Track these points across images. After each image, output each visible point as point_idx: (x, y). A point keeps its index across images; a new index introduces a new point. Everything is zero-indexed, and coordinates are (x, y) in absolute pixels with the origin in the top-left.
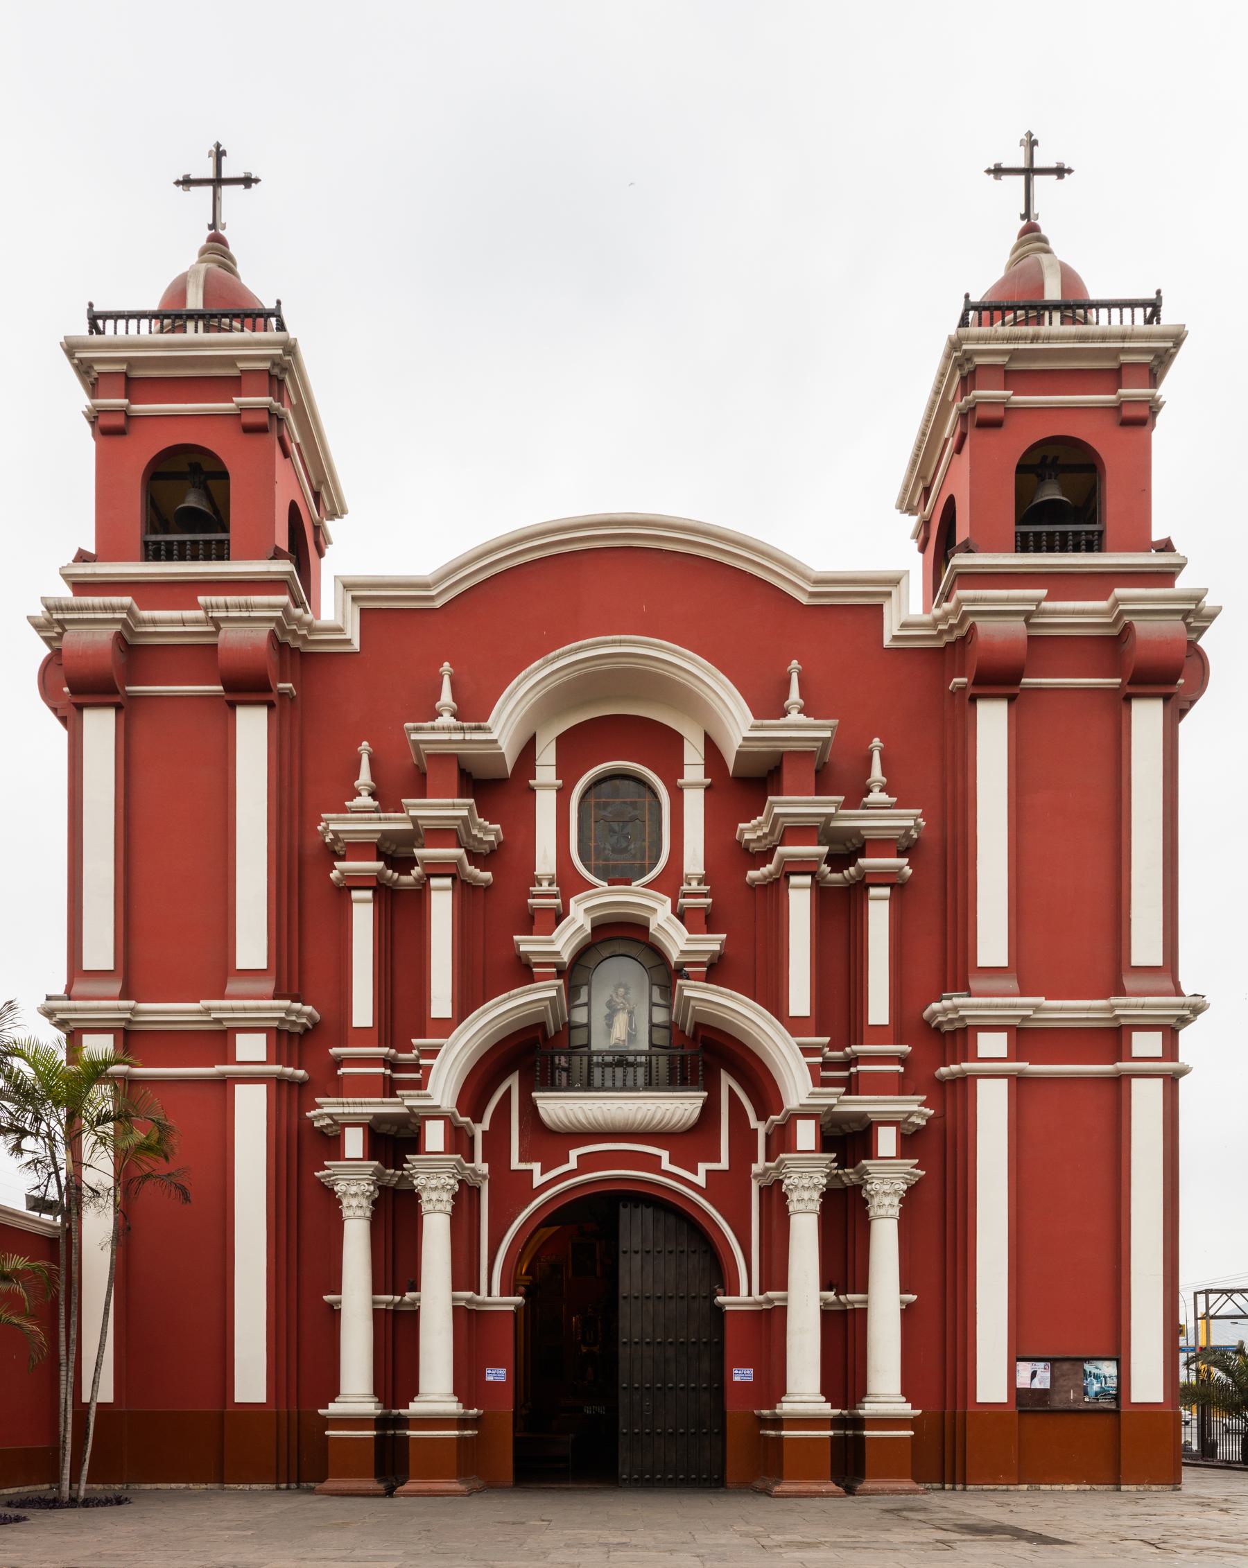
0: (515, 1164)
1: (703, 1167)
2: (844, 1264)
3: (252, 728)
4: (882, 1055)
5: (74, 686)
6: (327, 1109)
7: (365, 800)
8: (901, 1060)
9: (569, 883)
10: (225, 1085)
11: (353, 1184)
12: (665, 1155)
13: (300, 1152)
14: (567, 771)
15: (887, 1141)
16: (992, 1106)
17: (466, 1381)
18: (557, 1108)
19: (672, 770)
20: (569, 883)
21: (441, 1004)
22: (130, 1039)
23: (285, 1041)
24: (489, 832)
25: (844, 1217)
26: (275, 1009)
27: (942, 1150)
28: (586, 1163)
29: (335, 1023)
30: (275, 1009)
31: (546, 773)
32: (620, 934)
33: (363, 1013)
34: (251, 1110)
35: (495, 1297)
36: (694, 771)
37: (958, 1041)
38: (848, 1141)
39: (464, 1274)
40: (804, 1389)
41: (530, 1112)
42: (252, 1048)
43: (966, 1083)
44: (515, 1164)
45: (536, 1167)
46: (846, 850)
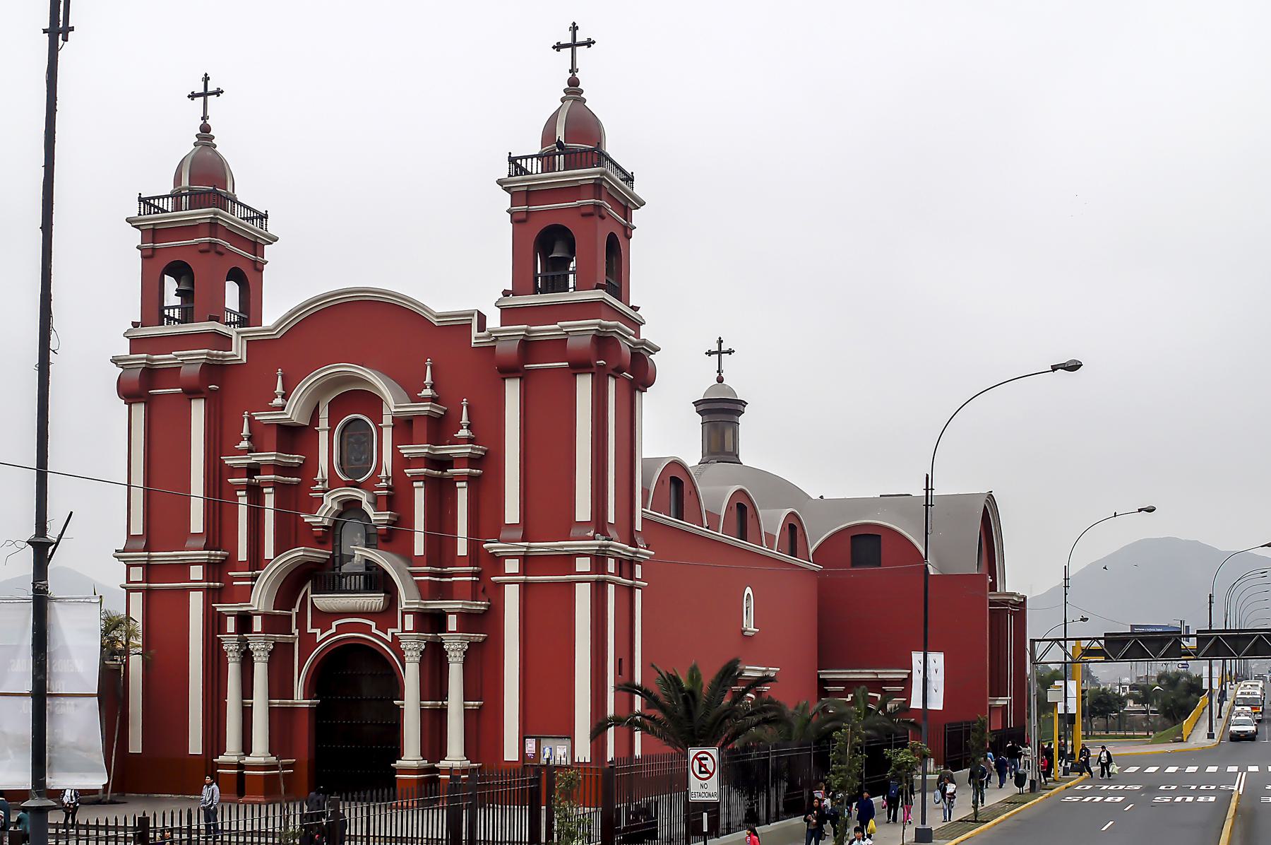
0: (310, 630)
1: (390, 631)
2: (434, 684)
3: (198, 410)
4: (462, 575)
5: (128, 393)
6: (221, 608)
7: (244, 444)
8: (473, 574)
10: (186, 591)
11: (230, 645)
12: (373, 624)
13: (214, 624)
14: (332, 424)
15: (452, 623)
16: (512, 595)
17: (275, 746)
18: (326, 602)
19: (378, 418)
20: (334, 482)
21: (269, 552)
22: (150, 570)
23: (213, 570)
24: (296, 459)
25: (434, 661)
26: (204, 555)
27: (484, 623)
28: (340, 629)
29: (230, 561)
30: (204, 555)
31: (324, 423)
33: (242, 555)
37: (497, 562)
38: (432, 622)
40: (411, 756)
42: (196, 573)
43: (501, 586)
44: (310, 630)
45: (318, 631)
46: (444, 463)
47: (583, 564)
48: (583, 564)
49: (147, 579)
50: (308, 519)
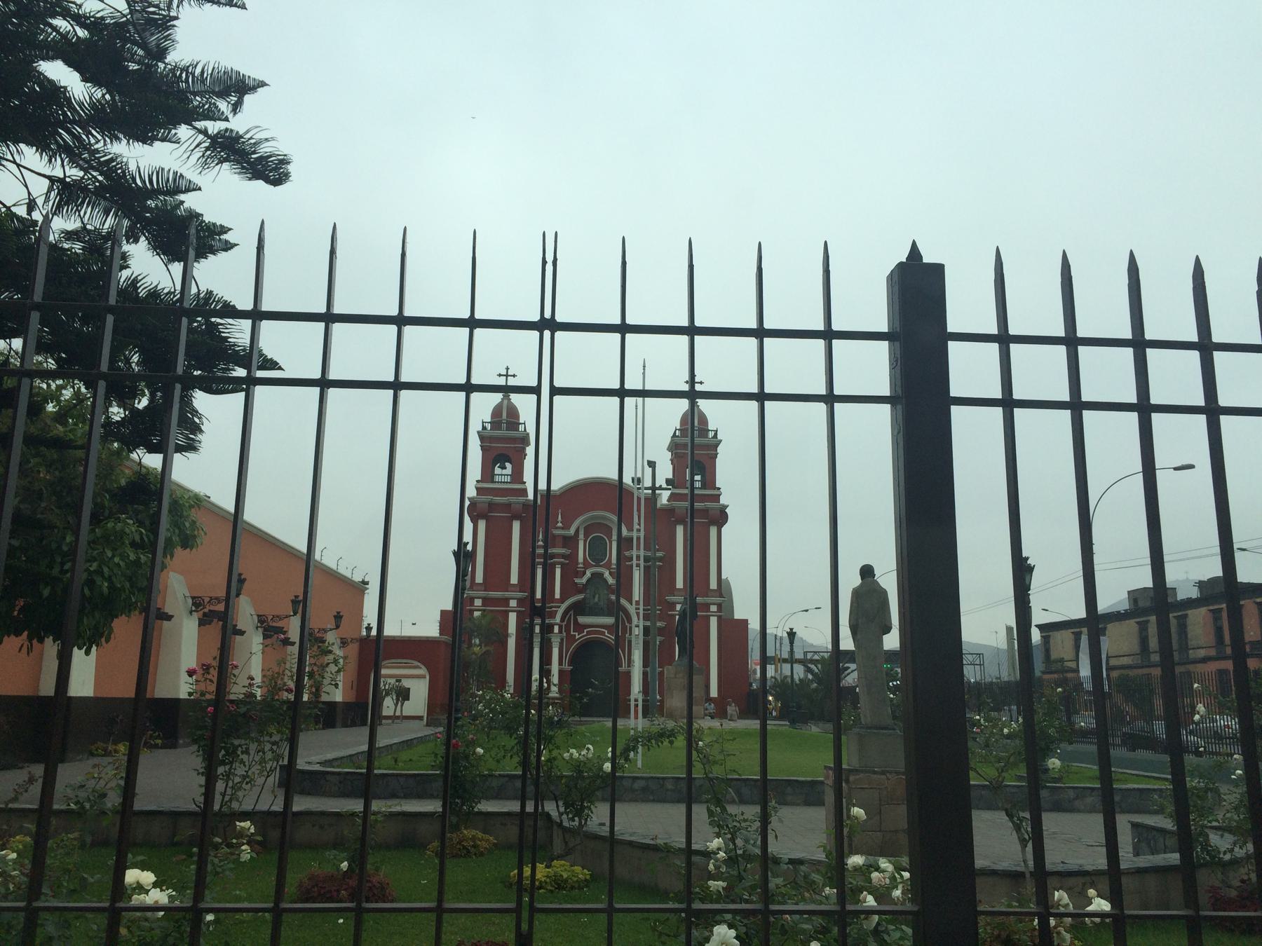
3: (516, 526)
9: (587, 565)
14: (586, 536)
19: (610, 537)
23: (521, 602)
26: (520, 595)
30: (520, 595)
31: (581, 536)
32: (597, 577)
34: (513, 618)
35: (567, 667)
36: (615, 537)
39: (560, 663)
41: (575, 620)
42: (513, 603)
47: (714, 608)
48: (714, 608)
49: (483, 605)
50: (577, 581)
